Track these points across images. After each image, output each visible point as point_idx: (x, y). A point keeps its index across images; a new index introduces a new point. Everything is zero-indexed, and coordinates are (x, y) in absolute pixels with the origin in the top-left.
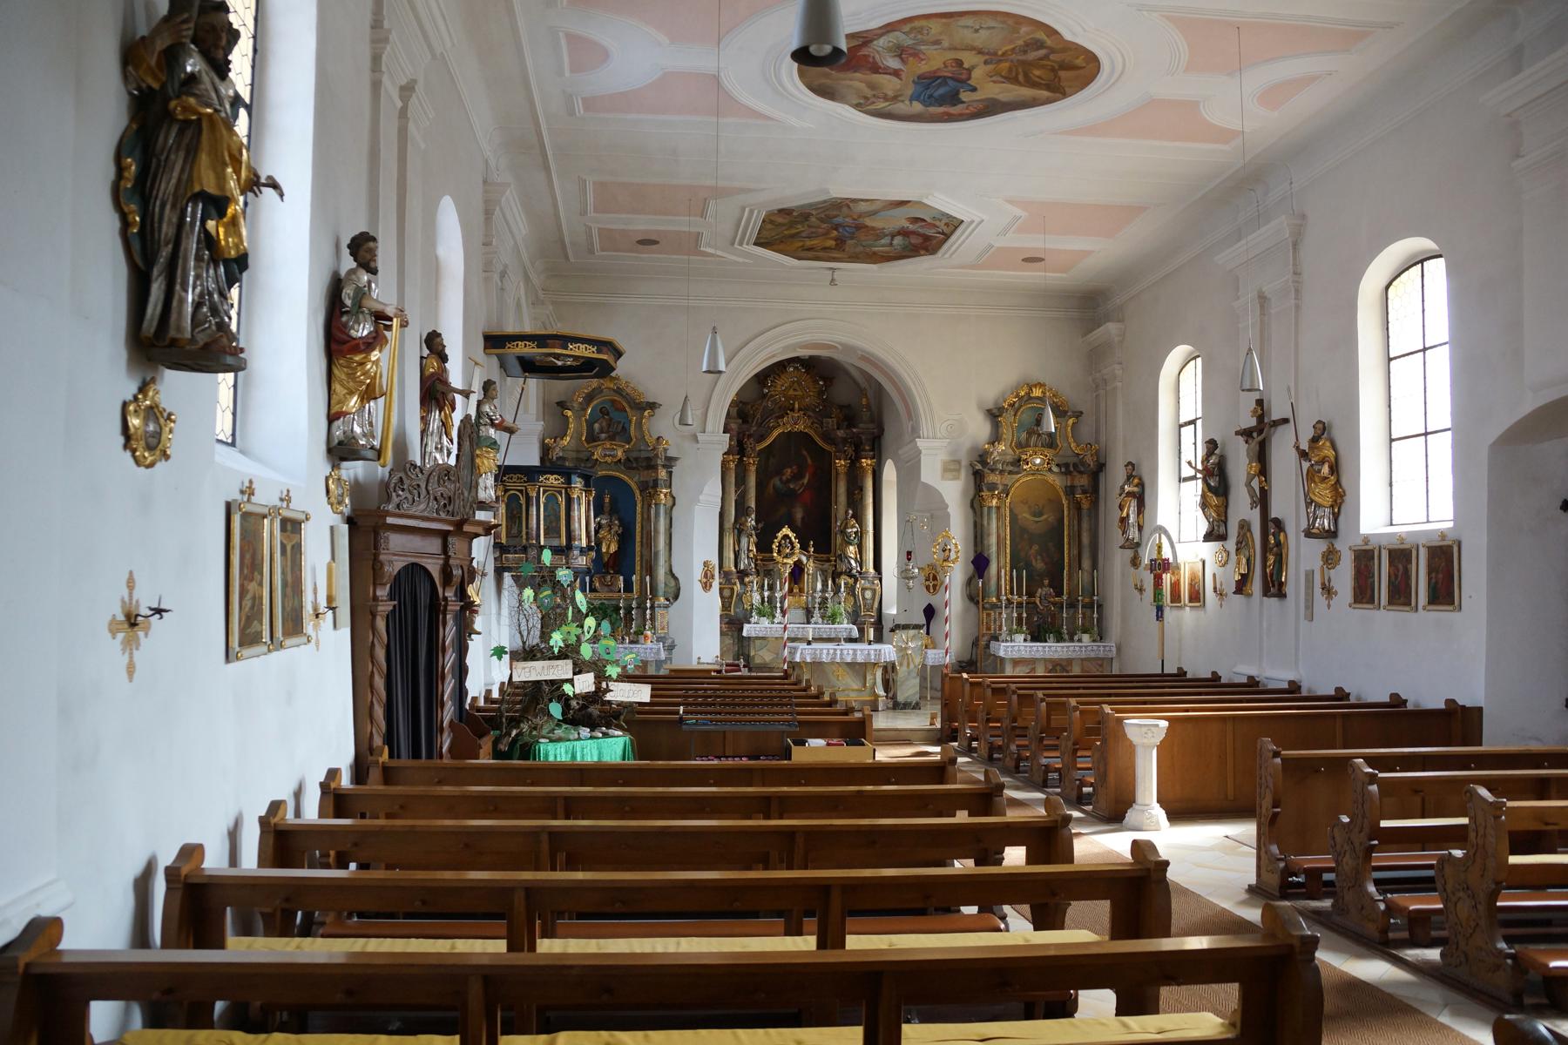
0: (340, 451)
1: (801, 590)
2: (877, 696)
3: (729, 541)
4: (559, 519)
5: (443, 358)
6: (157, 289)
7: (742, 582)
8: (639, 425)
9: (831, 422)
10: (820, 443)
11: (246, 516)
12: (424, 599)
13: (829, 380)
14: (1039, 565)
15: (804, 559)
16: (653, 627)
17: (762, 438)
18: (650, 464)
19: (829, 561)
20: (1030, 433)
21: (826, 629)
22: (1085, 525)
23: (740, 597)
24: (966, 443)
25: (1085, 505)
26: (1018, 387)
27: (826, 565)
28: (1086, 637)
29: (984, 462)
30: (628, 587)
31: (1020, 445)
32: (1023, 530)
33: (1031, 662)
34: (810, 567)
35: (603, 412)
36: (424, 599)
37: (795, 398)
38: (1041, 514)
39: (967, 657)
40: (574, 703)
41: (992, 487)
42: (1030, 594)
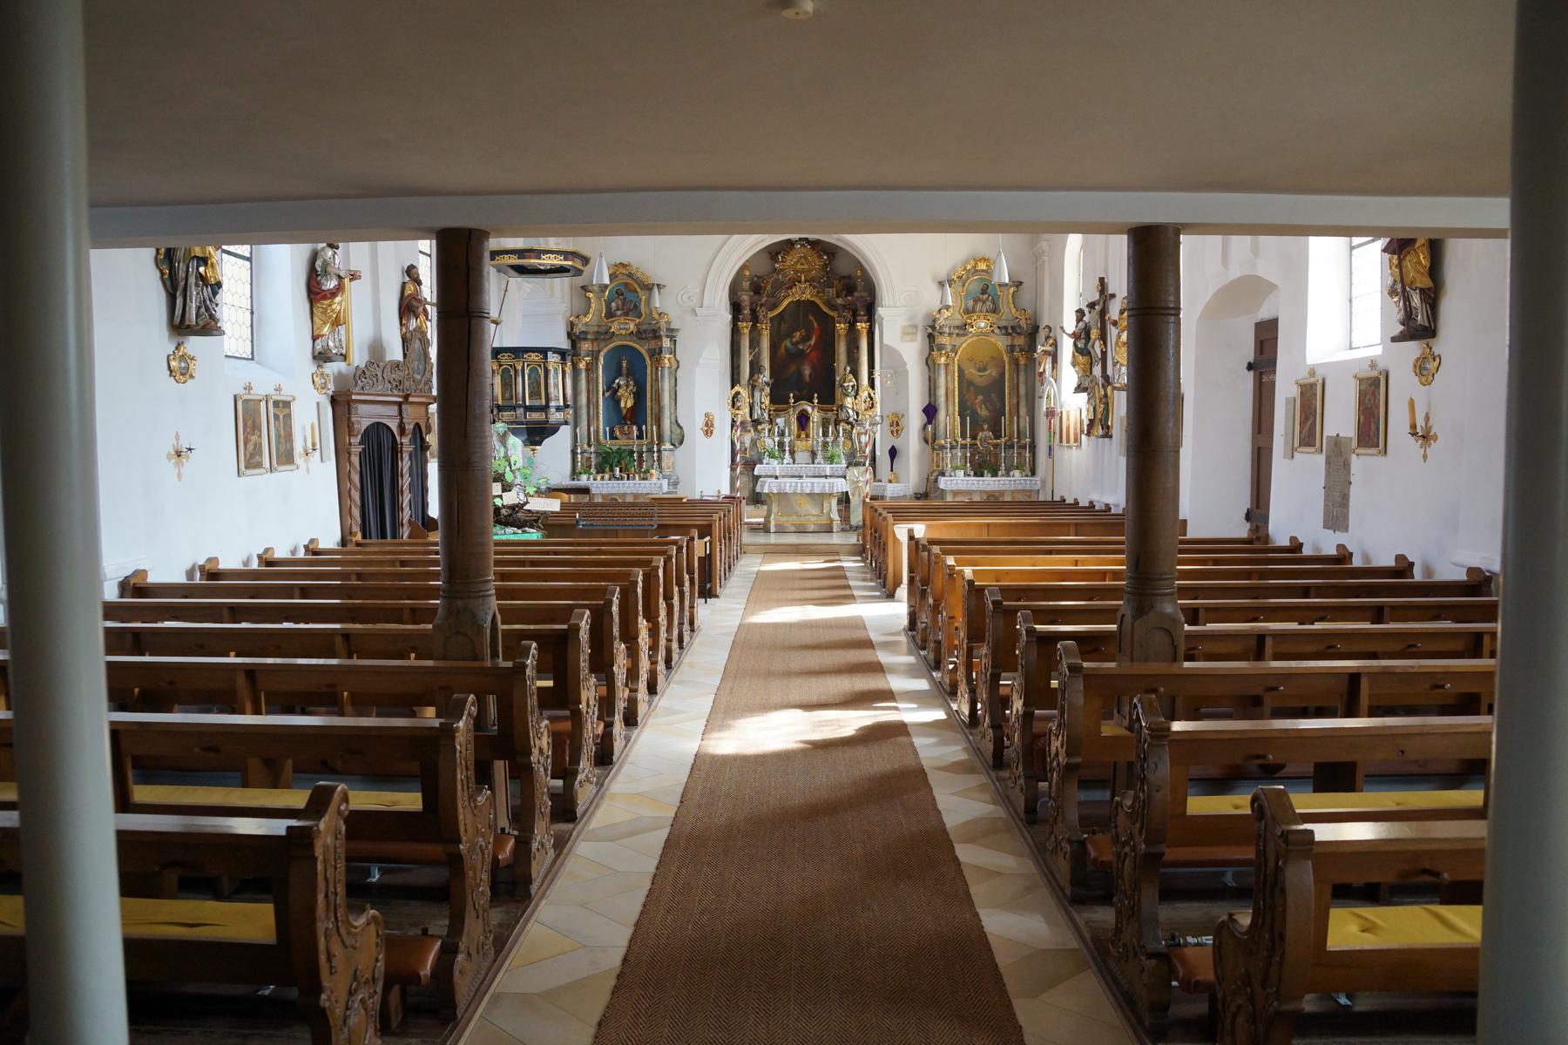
0: (321, 357)
2: (832, 520)
4: (539, 385)
5: (419, 283)
6: (179, 301)
7: (756, 430)
8: (648, 302)
9: (832, 292)
10: (825, 309)
11: (246, 401)
12: (387, 444)
14: (983, 412)
15: (809, 409)
16: (660, 466)
17: (775, 306)
18: (656, 336)
20: (976, 301)
21: (828, 469)
22: (1022, 379)
24: (922, 311)
25: (1022, 362)
26: (967, 261)
28: (1017, 473)
29: (933, 327)
30: (640, 437)
31: (967, 311)
32: (970, 383)
33: (969, 492)
34: (815, 416)
35: (619, 293)
36: (387, 444)
37: (803, 271)
38: (985, 370)
39: (922, 491)
40: (504, 511)
41: (941, 348)
42: (974, 437)
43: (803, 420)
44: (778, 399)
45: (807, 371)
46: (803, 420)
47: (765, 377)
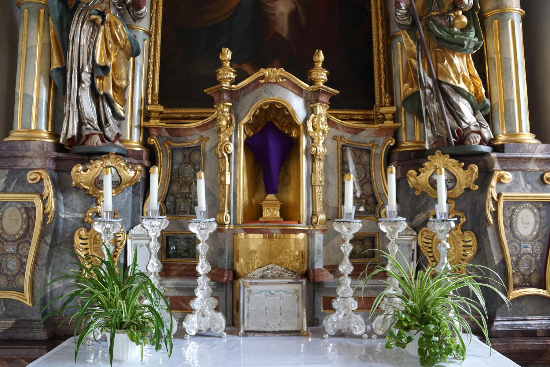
1: (288, 213)
7: (62, 185)
15: (297, 105)
23: (58, 239)
27: (367, 135)
43: (273, 149)
44: (183, 85)
46: (273, 149)
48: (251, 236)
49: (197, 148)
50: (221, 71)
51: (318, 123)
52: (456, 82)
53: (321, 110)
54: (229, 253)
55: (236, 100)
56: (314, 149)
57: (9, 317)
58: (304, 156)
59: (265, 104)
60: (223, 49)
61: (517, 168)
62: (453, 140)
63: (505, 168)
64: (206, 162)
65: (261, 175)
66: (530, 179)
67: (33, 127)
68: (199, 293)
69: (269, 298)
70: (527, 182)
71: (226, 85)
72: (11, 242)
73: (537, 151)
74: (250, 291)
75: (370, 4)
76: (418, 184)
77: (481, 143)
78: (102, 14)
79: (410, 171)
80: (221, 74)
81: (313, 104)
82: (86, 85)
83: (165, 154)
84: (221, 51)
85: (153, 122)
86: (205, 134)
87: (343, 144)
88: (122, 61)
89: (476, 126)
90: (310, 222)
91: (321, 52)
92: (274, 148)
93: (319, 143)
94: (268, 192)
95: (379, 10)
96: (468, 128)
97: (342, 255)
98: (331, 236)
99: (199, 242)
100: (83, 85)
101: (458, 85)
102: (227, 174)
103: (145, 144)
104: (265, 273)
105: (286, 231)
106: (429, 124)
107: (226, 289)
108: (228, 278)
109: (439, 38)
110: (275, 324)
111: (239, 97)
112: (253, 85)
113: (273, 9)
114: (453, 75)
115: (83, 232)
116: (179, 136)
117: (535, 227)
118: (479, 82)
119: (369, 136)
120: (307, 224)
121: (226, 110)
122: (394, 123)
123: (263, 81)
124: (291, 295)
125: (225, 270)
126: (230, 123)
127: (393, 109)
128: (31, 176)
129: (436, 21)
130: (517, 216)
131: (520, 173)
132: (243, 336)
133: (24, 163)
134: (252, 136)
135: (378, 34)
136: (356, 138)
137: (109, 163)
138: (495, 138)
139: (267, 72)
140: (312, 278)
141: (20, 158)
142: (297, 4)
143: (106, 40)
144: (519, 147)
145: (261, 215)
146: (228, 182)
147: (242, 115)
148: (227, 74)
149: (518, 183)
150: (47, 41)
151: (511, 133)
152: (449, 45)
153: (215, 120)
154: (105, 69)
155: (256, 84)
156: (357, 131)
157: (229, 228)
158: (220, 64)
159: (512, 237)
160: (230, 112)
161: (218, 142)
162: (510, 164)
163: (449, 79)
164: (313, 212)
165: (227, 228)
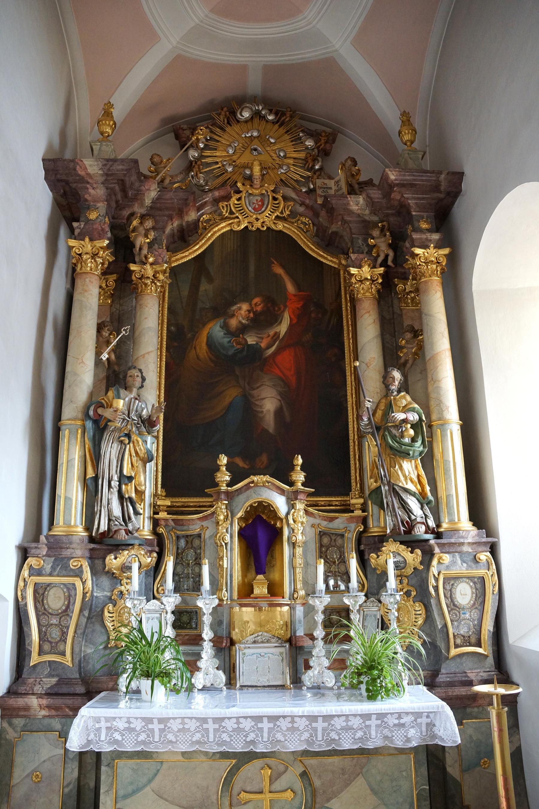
1: (274, 590)
3: (72, 455)
13: (326, 140)
15: (280, 503)
17: (184, 237)
19: (347, 509)
23: (94, 613)
27: (341, 522)
34: (298, 521)
43: (261, 537)
44: (185, 478)
45: (269, 403)
46: (261, 537)
47: (149, 395)
48: (244, 609)
49: (199, 536)
50: (219, 475)
51: (298, 517)
52: (405, 483)
53: (300, 506)
54: (226, 624)
55: (231, 499)
56: (294, 538)
57: (53, 676)
58: (286, 543)
59: (255, 503)
60: (220, 456)
61: (453, 551)
62: (402, 528)
63: (444, 551)
64: (206, 547)
65: (252, 558)
66: (465, 559)
67: (72, 524)
68: (204, 655)
69: (260, 660)
70: (463, 561)
71: (224, 488)
72: (55, 615)
73: (469, 536)
74: (244, 654)
75: (347, 400)
76: (378, 565)
77: (426, 532)
78: (128, 436)
79: (372, 555)
80: (219, 477)
81: (293, 501)
82: (115, 490)
83: (171, 540)
84: (218, 457)
85: (163, 515)
86: (205, 523)
87: (321, 530)
88: (141, 470)
89: (422, 517)
90: (292, 597)
91: (300, 456)
92: (262, 536)
93: (298, 533)
94: (258, 572)
95: (354, 405)
96: (416, 519)
97: (315, 622)
98: (310, 610)
99: (205, 614)
100: (112, 490)
101: (406, 486)
102: (225, 558)
103: (154, 532)
104: (256, 639)
105: (272, 605)
106: (389, 513)
107: (225, 654)
108: (226, 644)
109: (391, 448)
110: (265, 680)
111: (233, 496)
112: (245, 487)
113: (261, 407)
114: (402, 478)
115: (110, 606)
116: (183, 525)
117: (472, 597)
118: (425, 481)
119: (341, 523)
120: (290, 599)
121: (224, 507)
122: (363, 512)
123: (253, 485)
124: (277, 657)
125: (223, 637)
126: (226, 518)
127: (361, 501)
128: (73, 564)
129: (391, 431)
130: (455, 589)
131: (457, 554)
132: (239, 690)
133: (66, 553)
134: (244, 527)
135: (354, 428)
136: (331, 525)
137: (133, 552)
138: (438, 526)
139: (255, 478)
140: (294, 643)
141: (64, 548)
142: (282, 402)
143: (131, 455)
144: (455, 534)
145: (252, 592)
146: (225, 566)
147: (236, 511)
148: (224, 477)
149: (455, 562)
150: (83, 454)
151: (451, 521)
152: (399, 454)
153: (213, 513)
154: (130, 479)
155: (247, 487)
156: (332, 519)
157: (227, 603)
158: (217, 468)
159: (452, 606)
160: (226, 508)
161: (217, 534)
162: (446, 548)
163: (398, 481)
164: (294, 589)
165: (225, 603)
